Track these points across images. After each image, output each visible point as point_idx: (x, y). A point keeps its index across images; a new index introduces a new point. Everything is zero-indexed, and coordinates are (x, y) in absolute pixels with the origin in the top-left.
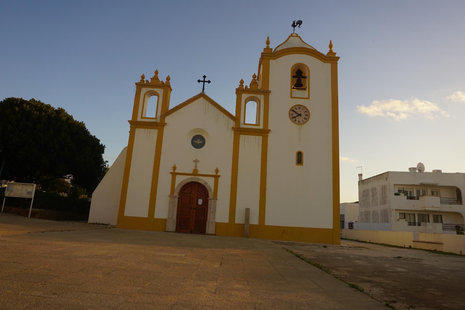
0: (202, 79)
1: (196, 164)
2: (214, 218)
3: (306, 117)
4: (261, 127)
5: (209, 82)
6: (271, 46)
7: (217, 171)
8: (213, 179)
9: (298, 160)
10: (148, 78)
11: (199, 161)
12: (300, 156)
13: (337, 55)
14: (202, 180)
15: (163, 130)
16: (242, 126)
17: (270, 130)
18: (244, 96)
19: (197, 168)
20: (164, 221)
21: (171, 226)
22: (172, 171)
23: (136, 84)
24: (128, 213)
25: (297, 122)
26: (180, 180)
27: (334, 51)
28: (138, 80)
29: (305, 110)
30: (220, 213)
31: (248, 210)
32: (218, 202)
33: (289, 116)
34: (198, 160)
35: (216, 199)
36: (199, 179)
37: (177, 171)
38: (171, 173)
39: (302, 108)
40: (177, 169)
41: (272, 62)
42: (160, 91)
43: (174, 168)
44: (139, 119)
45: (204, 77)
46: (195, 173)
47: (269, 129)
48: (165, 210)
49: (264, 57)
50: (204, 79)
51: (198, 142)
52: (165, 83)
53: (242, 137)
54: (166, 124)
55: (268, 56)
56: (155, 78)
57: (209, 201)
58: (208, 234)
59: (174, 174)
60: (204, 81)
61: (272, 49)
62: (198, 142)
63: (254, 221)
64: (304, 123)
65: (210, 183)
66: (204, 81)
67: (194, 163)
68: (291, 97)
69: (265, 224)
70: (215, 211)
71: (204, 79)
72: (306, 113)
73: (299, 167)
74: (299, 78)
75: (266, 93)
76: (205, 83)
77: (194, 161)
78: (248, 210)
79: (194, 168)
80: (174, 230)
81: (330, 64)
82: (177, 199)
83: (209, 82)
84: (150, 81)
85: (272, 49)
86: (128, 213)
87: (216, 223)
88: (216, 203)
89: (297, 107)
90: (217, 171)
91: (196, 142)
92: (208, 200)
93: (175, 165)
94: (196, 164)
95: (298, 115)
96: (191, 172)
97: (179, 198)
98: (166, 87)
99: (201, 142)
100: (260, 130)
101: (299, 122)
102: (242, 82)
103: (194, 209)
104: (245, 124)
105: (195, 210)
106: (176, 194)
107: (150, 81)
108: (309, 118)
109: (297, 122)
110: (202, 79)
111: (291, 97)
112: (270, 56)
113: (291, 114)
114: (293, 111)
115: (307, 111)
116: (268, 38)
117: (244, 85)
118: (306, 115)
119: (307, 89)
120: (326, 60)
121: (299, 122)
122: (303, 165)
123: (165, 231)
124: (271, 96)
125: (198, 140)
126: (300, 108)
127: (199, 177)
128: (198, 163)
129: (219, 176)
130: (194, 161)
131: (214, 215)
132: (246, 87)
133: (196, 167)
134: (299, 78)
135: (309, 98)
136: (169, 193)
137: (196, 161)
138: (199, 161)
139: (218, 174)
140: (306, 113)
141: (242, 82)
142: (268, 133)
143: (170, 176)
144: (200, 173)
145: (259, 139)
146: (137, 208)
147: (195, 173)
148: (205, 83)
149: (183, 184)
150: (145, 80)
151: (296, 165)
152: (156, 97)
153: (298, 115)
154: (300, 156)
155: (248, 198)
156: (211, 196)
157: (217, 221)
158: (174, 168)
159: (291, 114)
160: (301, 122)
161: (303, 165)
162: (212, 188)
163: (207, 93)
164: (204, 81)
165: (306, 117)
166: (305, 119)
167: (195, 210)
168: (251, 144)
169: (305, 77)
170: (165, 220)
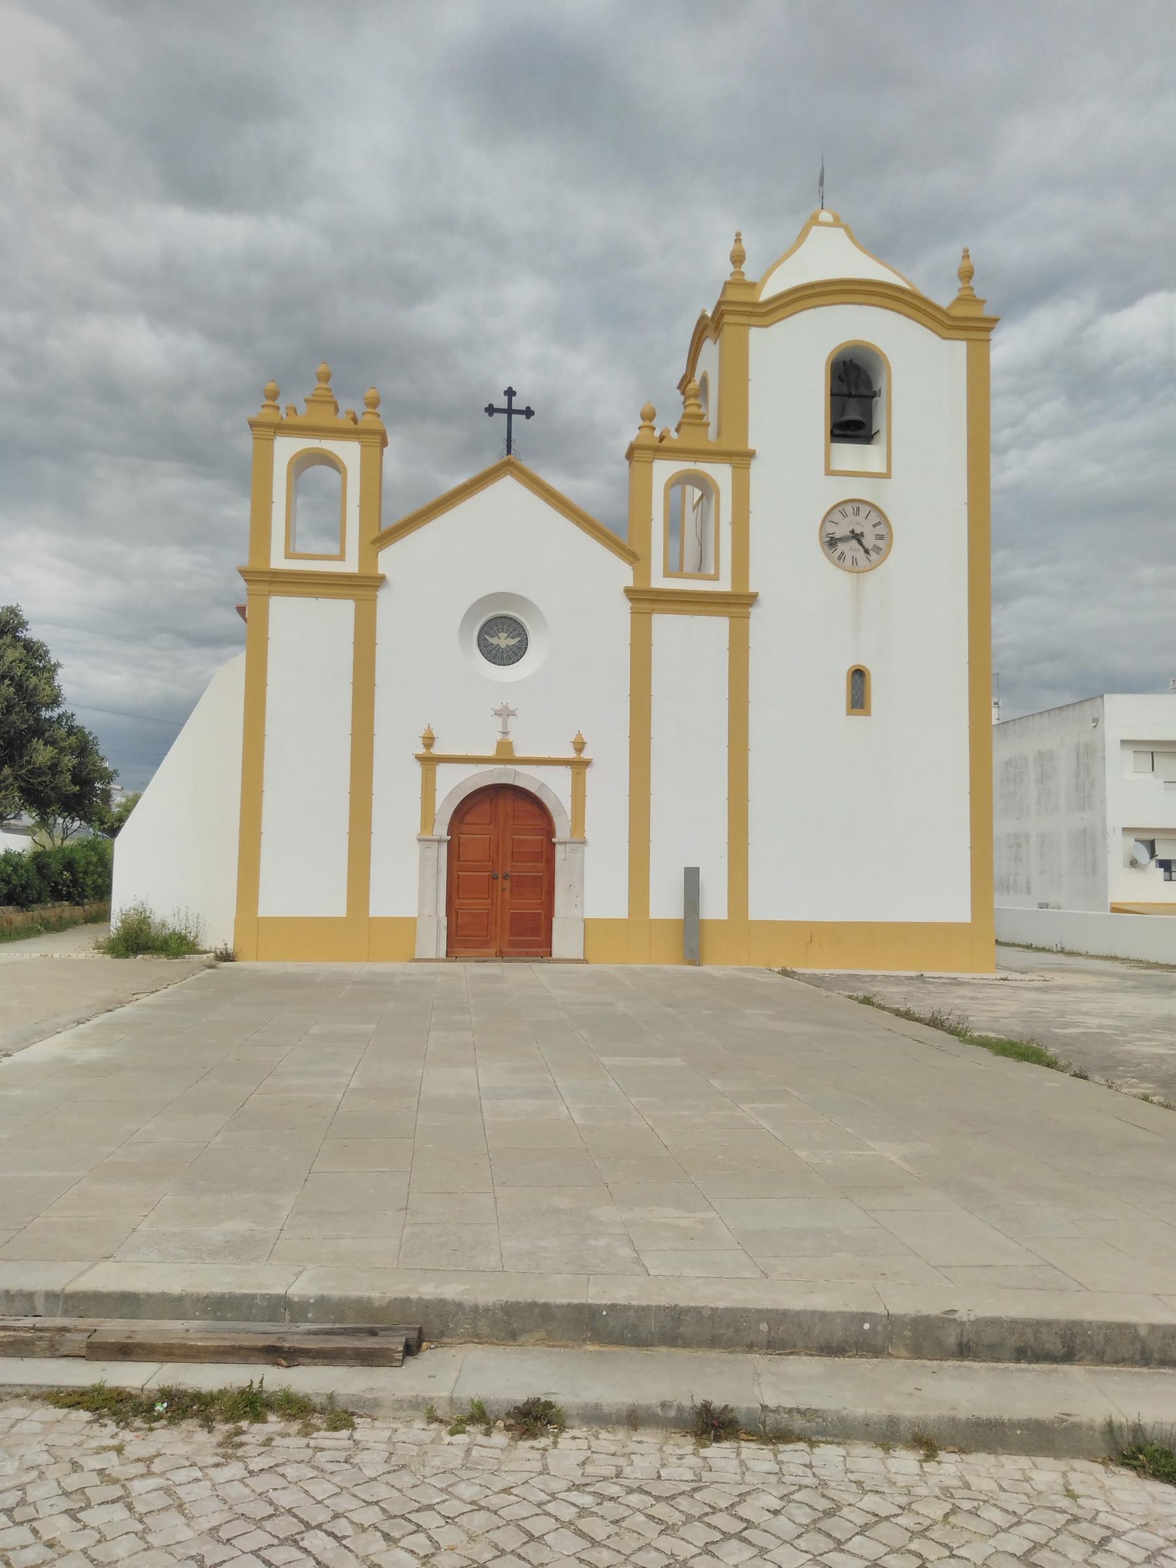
0: (502, 402)
1: (505, 724)
4: (724, 585)
5: (528, 413)
7: (580, 746)
8: (566, 773)
13: (987, 312)
14: (528, 778)
15: (374, 600)
16: (659, 581)
17: (754, 596)
19: (511, 738)
20: (406, 926)
22: (421, 750)
25: (848, 561)
27: (979, 293)
29: (874, 518)
31: (692, 876)
35: (583, 842)
36: (516, 773)
37: (437, 750)
38: (420, 758)
39: (864, 510)
40: (436, 743)
41: (755, 334)
43: (429, 741)
46: (505, 755)
48: (409, 884)
50: (510, 402)
51: (503, 641)
58: (559, 961)
59: (429, 761)
62: (503, 641)
67: (499, 720)
68: (829, 472)
71: (510, 402)
72: (880, 530)
73: (858, 721)
74: (854, 399)
77: (498, 714)
78: (692, 876)
79: (499, 737)
80: (443, 954)
89: (849, 509)
90: (580, 746)
91: (494, 641)
94: (505, 724)
95: (854, 538)
96: (491, 752)
103: (505, 877)
105: (507, 883)
109: (848, 561)
110: (502, 402)
111: (829, 472)
115: (883, 520)
116: (738, 240)
118: (880, 537)
119: (882, 437)
120: (951, 328)
122: (869, 714)
124: (755, 467)
125: (503, 635)
126: (857, 512)
127: (520, 768)
129: (587, 763)
130: (498, 714)
133: (505, 733)
134: (854, 399)
135: (887, 476)
137: (505, 713)
139: (585, 755)
140: (880, 530)
142: (751, 605)
143: (417, 769)
144: (519, 753)
145: (717, 627)
146: (303, 883)
147: (505, 755)
153: (854, 538)
156: (562, 831)
158: (429, 741)
161: (869, 714)
162: (567, 804)
167: (507, 883)
168: (690, 647)
169: (874, 395)
170: (413, 921)
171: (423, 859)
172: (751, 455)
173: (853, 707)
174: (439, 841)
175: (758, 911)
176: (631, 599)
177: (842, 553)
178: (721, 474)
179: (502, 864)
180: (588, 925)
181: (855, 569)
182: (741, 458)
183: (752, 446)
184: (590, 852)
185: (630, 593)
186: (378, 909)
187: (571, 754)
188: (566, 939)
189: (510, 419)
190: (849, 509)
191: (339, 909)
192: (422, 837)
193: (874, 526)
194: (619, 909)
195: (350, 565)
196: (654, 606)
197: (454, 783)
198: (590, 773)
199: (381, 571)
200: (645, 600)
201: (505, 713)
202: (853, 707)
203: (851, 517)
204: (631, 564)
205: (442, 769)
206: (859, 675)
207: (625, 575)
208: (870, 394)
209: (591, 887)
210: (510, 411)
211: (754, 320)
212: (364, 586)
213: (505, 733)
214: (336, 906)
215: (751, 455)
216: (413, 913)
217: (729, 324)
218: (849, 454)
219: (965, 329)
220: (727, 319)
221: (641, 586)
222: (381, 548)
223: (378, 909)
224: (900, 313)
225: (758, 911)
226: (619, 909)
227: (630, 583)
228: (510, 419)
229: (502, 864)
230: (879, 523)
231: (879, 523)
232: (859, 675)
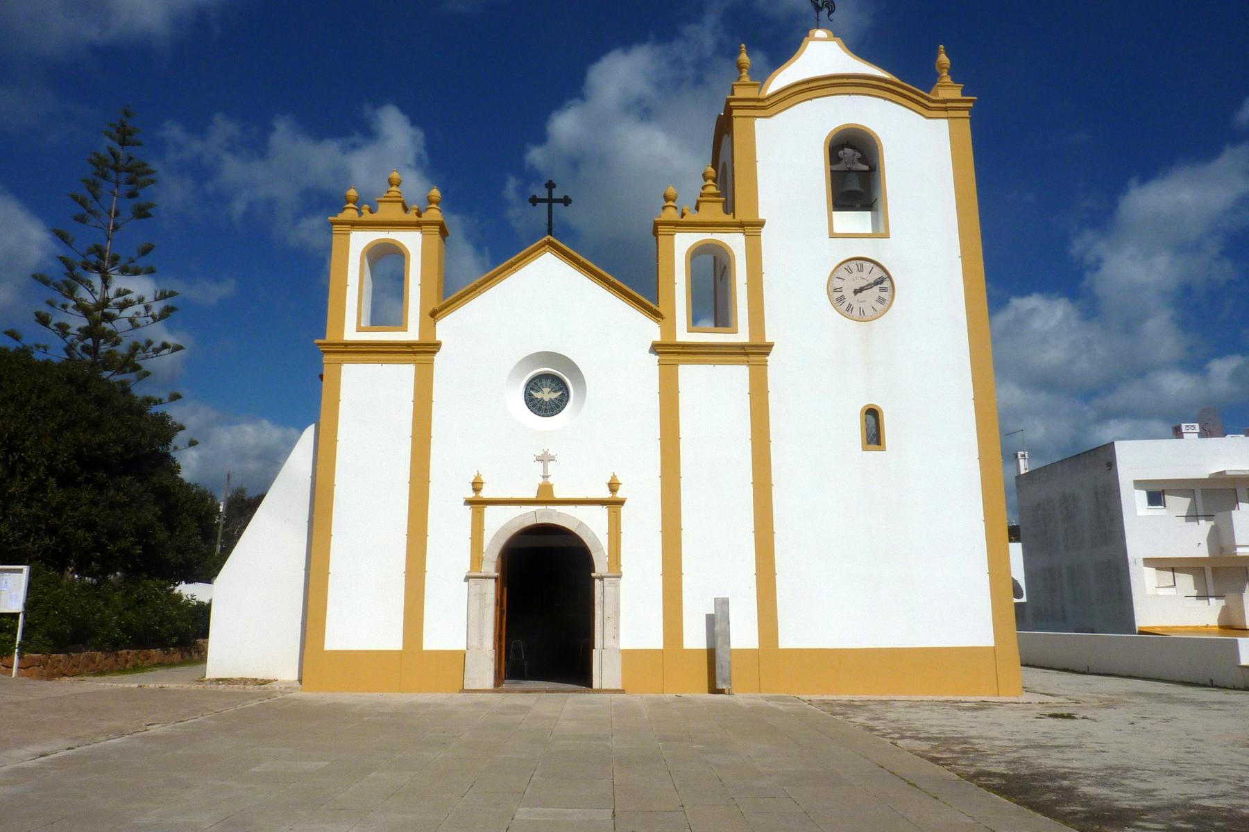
2: (616, 637)
4: (742, 336)
7: (613, 486)
8: (603, 511)
9: (868, 435)
15: (431, 363)
16: (683, 335)
17: (770, 346)
19: (550, 480)
20: (458, 659)
21: (482, 670)
22: (471, 495)
25: (856, 312)
32: (622, 581)
34: (551, 453)
37: (485, 494)
38: (469, 502)
41: (762, 126)
43: (477, 485)
46: (545, 498)
47: (768, 340)
50: (550, 194)
51: (546, 395)
53: (690, 375)
54: (438, 345)
57: (597, 582)
58: (600, 691)
59: (477, 504)
60: (550, 201)
62: (546, 395)
63: (743, 634)
64: (878, 315)
65: (590, 525)
67: (541, 465)
68: (833, 235)
71: (550, 194)
73: (874, 455)
79: (541, 480)
81: (946, 121)
83: (566, 201)
88: (617, 586)
90: (613, 486)
91: (538, 395)
93: (478, 477)
96: (532, 495)
99: (555, 396)
101: (862, 312)
106: (490, 567)
109: (856, 312)
111: (833, 235)
112: (755, 108)
113: (836, 290)
114: (879, 282)
119: (880, 204)
121: (862, 312)
123: (463, 690)
125: (546, 390)
126: (861, 269)
128: (551, 464)
129: (621, 503)
136: (465, 567)
137: (545, 459)
143: (468, 510)
144: (558, 494)
146: (363, 620)
147: (545, 498)
149: (508, 535)
151: (864, 450)
156: (601, 566)
157: (626, 643)
158: (477, 485)
159: (836, 290)
162: (604, 541)
166: (881, 300)
168: (714, 391)
170: (462, 655)
172: (761, 224)
173: (869, 443)
178: (735, 242)
179: (544, 595)
181: (862, 317)
182: (752, 227)
185: (656, 348)
186: (431, 642)
187: (606, 494)
188: (606, 669)
189: (550, 208)
190: (853, 265)
194: (654, 640)
195: (411, 334)
197: (501, 524)
199: (438, 339)
201: (545, 459)
202: (869, 443)
203: (856, 273)
205: (489, 510)
206: (872, 414)
207: (652, 331)
208: (866, 168)
209: (628, 619)
210: (550, 201)
214: (394, 643)
215: (761, 224)
216: (462, 646)
219: (946, 109)
220: (735, 113)
223: (431, 642)
224: (886, 99)
225: (787, 640)
226: (654, 640)
228: (550, 208)
229: (544, 595)
232: (872, 414)
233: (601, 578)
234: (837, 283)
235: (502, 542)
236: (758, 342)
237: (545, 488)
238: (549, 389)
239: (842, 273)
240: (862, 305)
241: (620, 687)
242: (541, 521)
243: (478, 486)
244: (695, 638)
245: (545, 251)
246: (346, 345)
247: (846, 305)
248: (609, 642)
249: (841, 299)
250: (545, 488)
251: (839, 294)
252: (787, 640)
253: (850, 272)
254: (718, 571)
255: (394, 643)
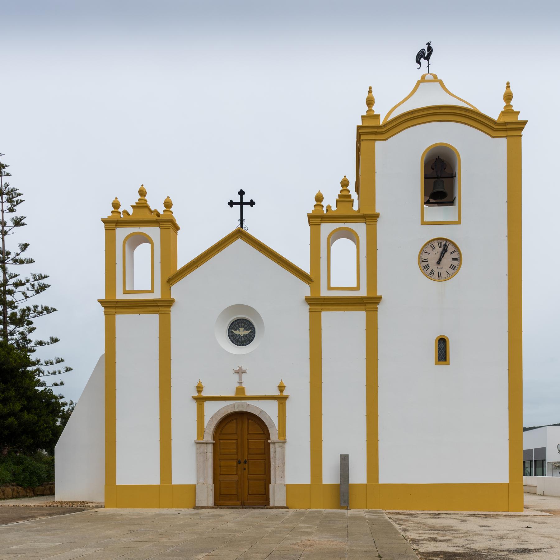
1: (240, 378)
2: (283, 477)
3: (455, 263)
4: (363, 293)
6: (376, 109)
7: (281, 388)
9: (439, 355)
10: (127, 206)
11: (244, 372)
12: (442, 344)
14: (254, 407)
16: (325, 293)
17: (380, 298)
18: (327, 228)
19: (243, 385)
21: (206, 496)
22: (196, 394)
23: (104, 221)
24: (123, 478)
25: (436, 275)
26: (213, 411)
28: (107, 212)
30: (292, 467)
32: (287, 446)
33: (420, 265)
34: (244, 368)
37: (204, 394)
38: (195, 398)
40: (204, 390)
41: (379, 145)
42: (154, 232)
43: (199, 389)
44: (120, 296)
45: (241, 193)
46: (240, 395)
48: (191, 468)
49: (362, 137)
52: (162, 213)
53: (329, 317)
55: (371, 132)
56: (141, 205)
57: (272, 446)
59: (200, 400)
61: (378, 116)
63: (358, 476)
64: (450, 276)
65: (269, 411)
66: (242, 203)
67: (236, 377)
68: (423, 223)
69: (381, 482)
70: (284, 463)
73: (442, 368)
75: (370, 218)
76: (244, 206)
79: (237, 385)
80: (211, 502)
82: (210, 448)
83: (252, 203)
84: (131, 211)
85: (378, 116)
86: (123, 478)
87: (288, 487)
88: (283, 448)
92: (269, 444)
94: (240, 378)
96: (232, 394)
97: (214, 444)
98: (167, 223)
100: (362, 298)
102: (319, 199)
104: (330, 289)
106: (208, 437)
107: (131, 211)
108: (460, 265)
109: (436, 275)
112: (376, 133)
117: (325, 203)
118: (454, 260)
121: (440, 275)
124: (380, 223)
128: (244, 375)
129: (286, 398)
131: (283, 472)
132: (329, 207)
133: (240, 383)
135: (459, 223)
136: (195, 437)
137: (240, 372)
138: (244, 372)
139: (285, 393)
141: (319, 199)
142: (378, 303)
143: (194, 404)
144: (248, 394)
145: (359, 317)
146: (137, 467)
147: (240, 395)
148: (244, 206)
149: (219, 418)
150: (121, 210)
152: (148, 245)
154: (442, 344)
155: (344, 436)
156: (274, 437)
157: (289, 480)
158: (199, 389)
159: (424, 260)
160: (444, 275)
162: (276, 421)
163: (250, 229)
164: (242, 202)
165: (455, 263)
166: (453, 267)
168: (343, 330)
170: (194, 487)
171: (198, 454)
172: (377, 216)
174: (207, 443)
175: (384, 478)
176: (309, 304)
177: (432, 270)
178: (360, 228)
180: (289, 488)
183: (377, 211)
184: (289, 448)
187: (277, 393)
191: (155, 480)
192: (197, 441)
193: (451, 253)
196: (323, 307)
198: (288, 403)
200: (317, 304)
204: (309, 284)
205: (207, 404)
206: (442, 343)
207: (306, 290)
211: (377, 137)
212: (162, 306)
213: (240, 383)
215: (377, 216)
216: (193, 482)
217: (363, 140)
218: (436, 213)
221: (316, 296)
222: (172, 284)
225: (384, 478)
227: (309, 294)
230: (454, 252)
231: (454, 252)
232: (442, 343)
233: (274, 443)
234: (425, 256)
235: (215, 422)
236: (372, 295)
237: (240, 390)
238: (242, 330)
239: (429, 249)
240: (440, 270)
241: (285, 505)
242: (237, 410)
243: (200, 389)
244: (330, 476)
245: (238, 238)
246: (118, 302)
247: (429, 271)
248: (279, 481)
249: (427, 267)
250: (240, 390)
251: (425, 264)
252: (383, 480)
253: (433, 248)
254: (344, 436)
255: (155, 480)
